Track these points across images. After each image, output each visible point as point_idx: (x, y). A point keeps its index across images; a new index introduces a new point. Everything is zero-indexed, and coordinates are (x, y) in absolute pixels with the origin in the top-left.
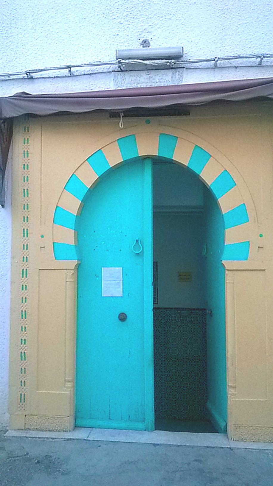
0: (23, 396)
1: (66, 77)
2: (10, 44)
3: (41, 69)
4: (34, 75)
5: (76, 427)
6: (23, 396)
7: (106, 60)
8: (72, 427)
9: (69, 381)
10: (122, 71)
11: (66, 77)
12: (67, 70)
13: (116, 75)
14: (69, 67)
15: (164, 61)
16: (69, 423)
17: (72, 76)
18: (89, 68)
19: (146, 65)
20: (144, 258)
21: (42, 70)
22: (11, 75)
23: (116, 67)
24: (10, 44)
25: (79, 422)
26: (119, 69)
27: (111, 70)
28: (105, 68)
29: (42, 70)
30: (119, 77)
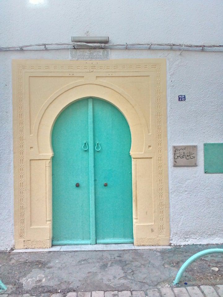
0: (72, 67)
1: (43, 50)
2: (9, 29)
3: (28, 45)
4: (24, 48)
5: (53, 246)
6: (72, 67)
7: (67, 42)
8: (51, 245)
9: (49, 221)
10: (75, 48)
11: (43, 50)
12: (44, 46)
13: (72, 51)
14: (45, 45)
15: (99, 44)
16: (49, 243)
17: (46, 50)
18: (56, 46)
19: (88, 46)
20: (89, 154)
21: (28, 46)
22: (10, 48)
23: (71, 47)
24: (9, 29)
25: (55, 243)
26: (74, 48)
27: (69, 47)
28: (65, 46)
29: (28, 46)
30: (74, 52)
